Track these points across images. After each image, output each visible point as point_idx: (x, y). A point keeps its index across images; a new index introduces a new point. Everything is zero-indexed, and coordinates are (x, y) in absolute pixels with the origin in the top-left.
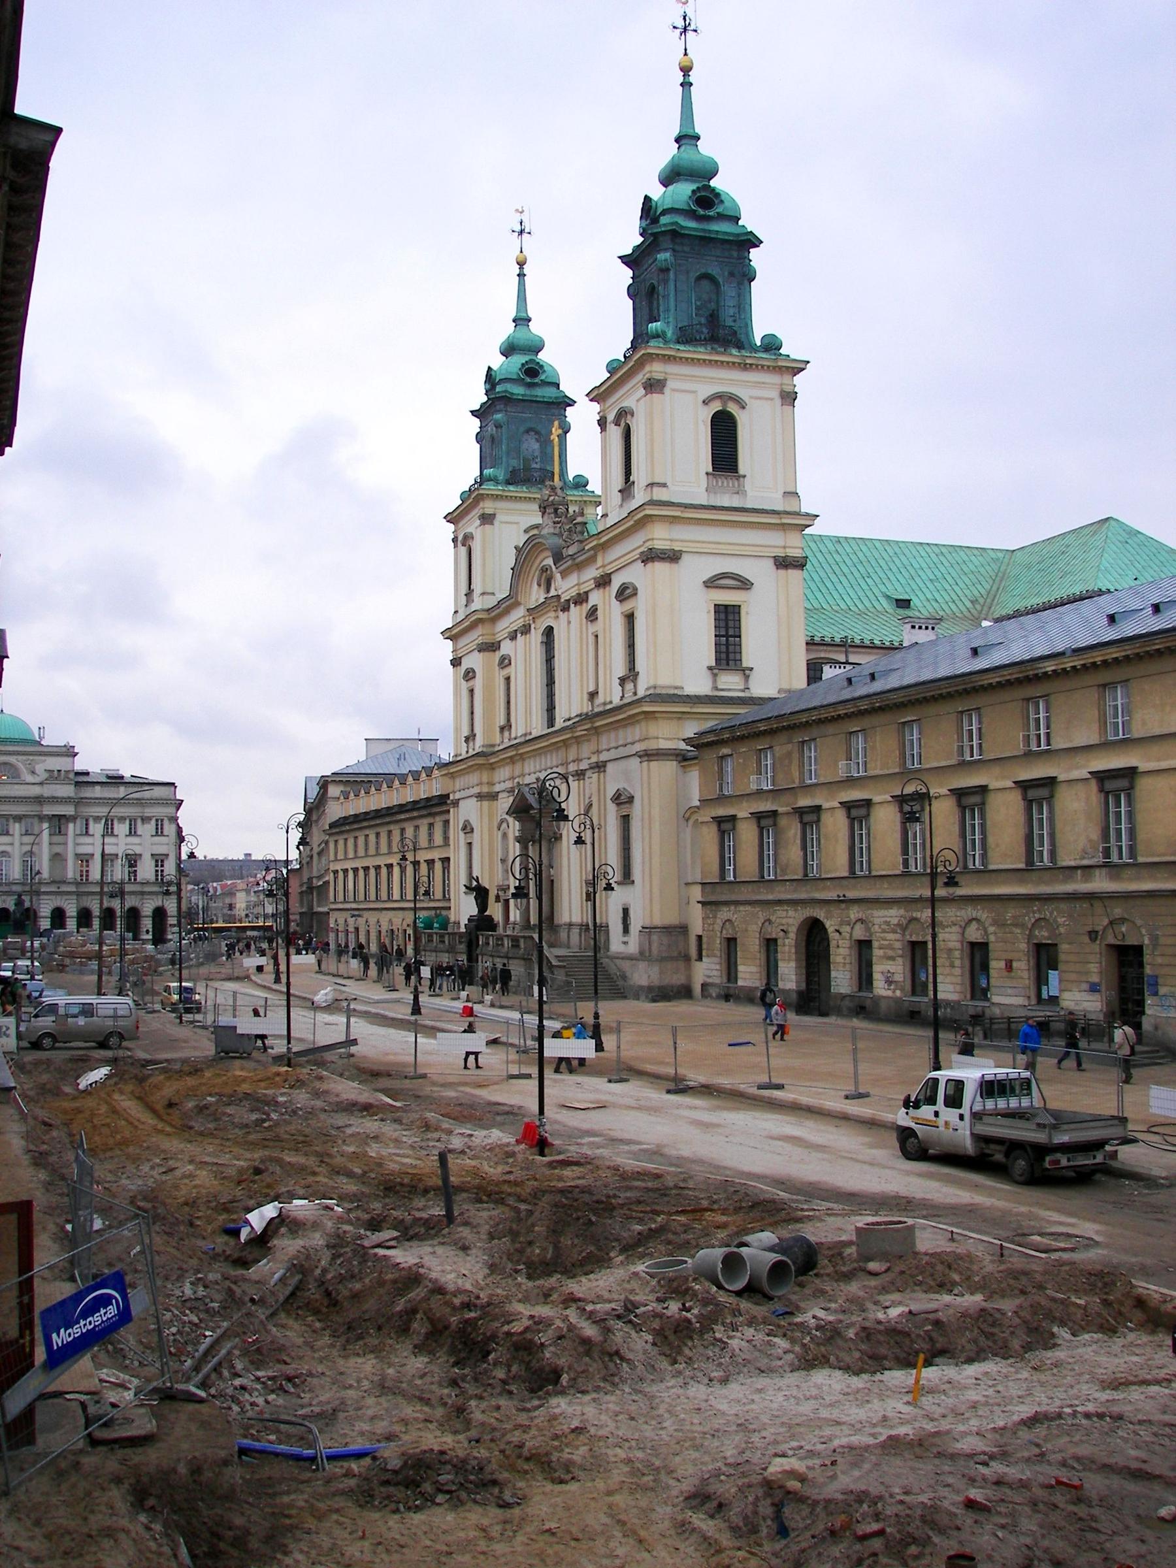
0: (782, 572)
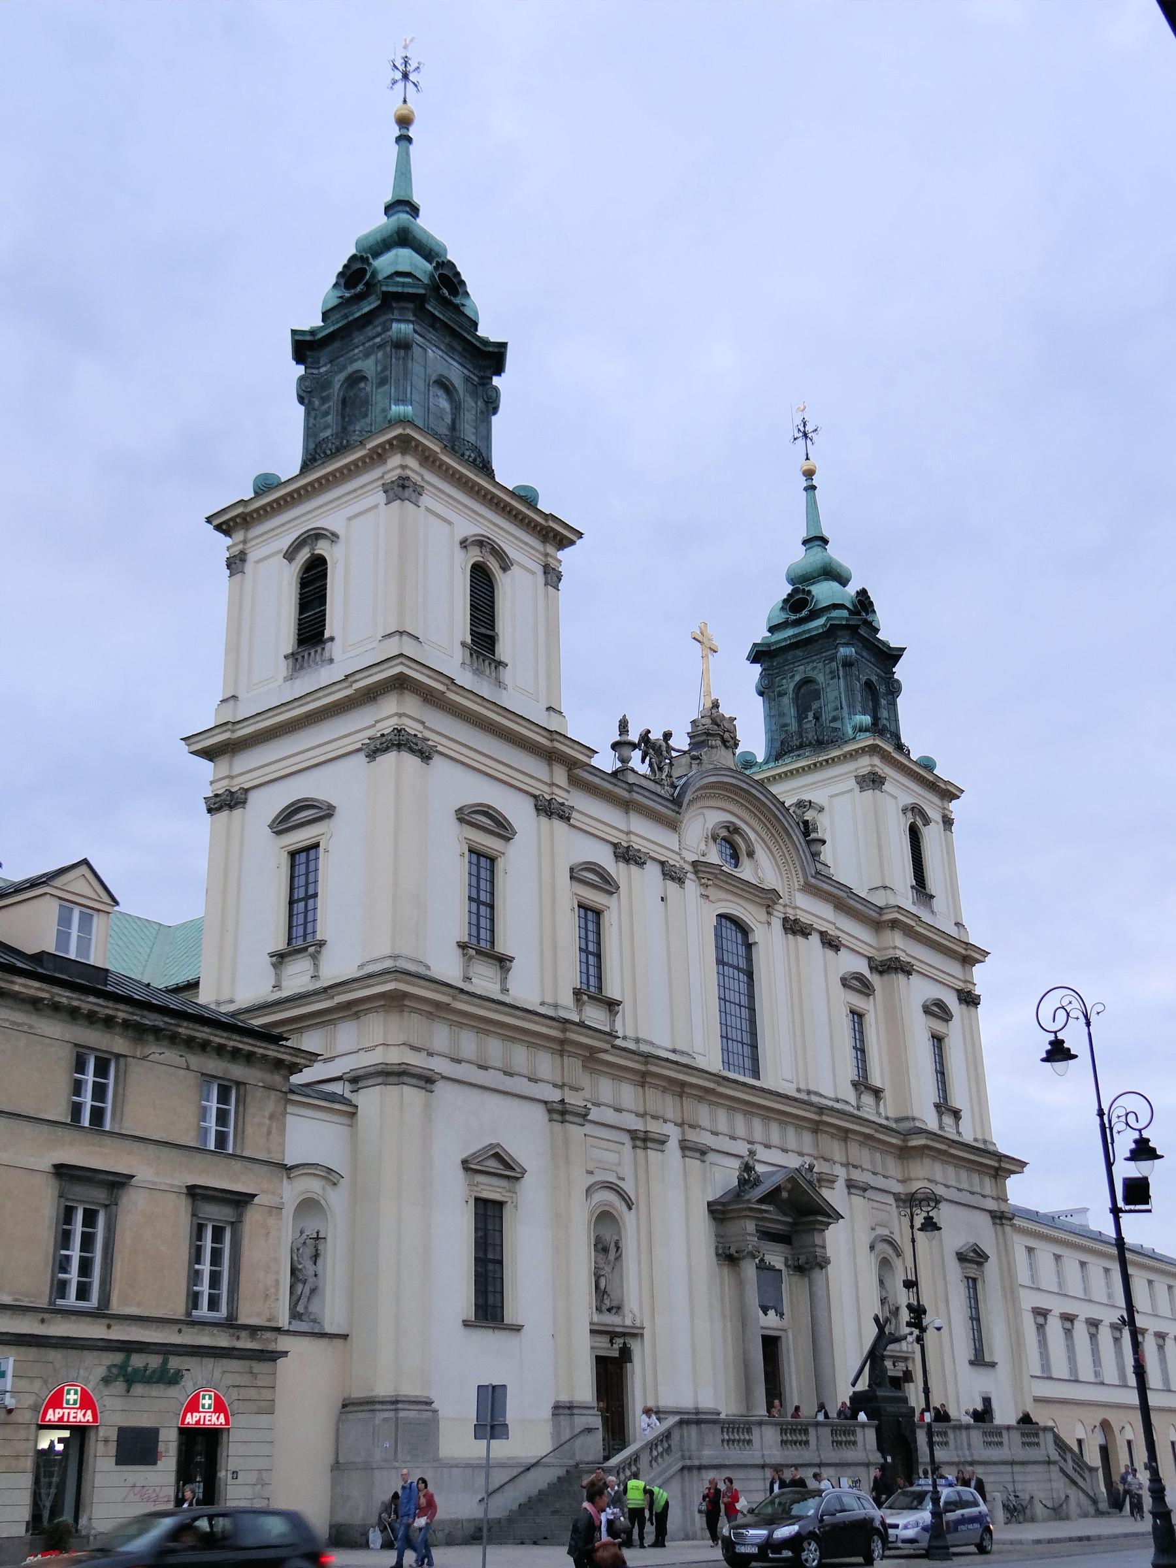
0: (544, 820)
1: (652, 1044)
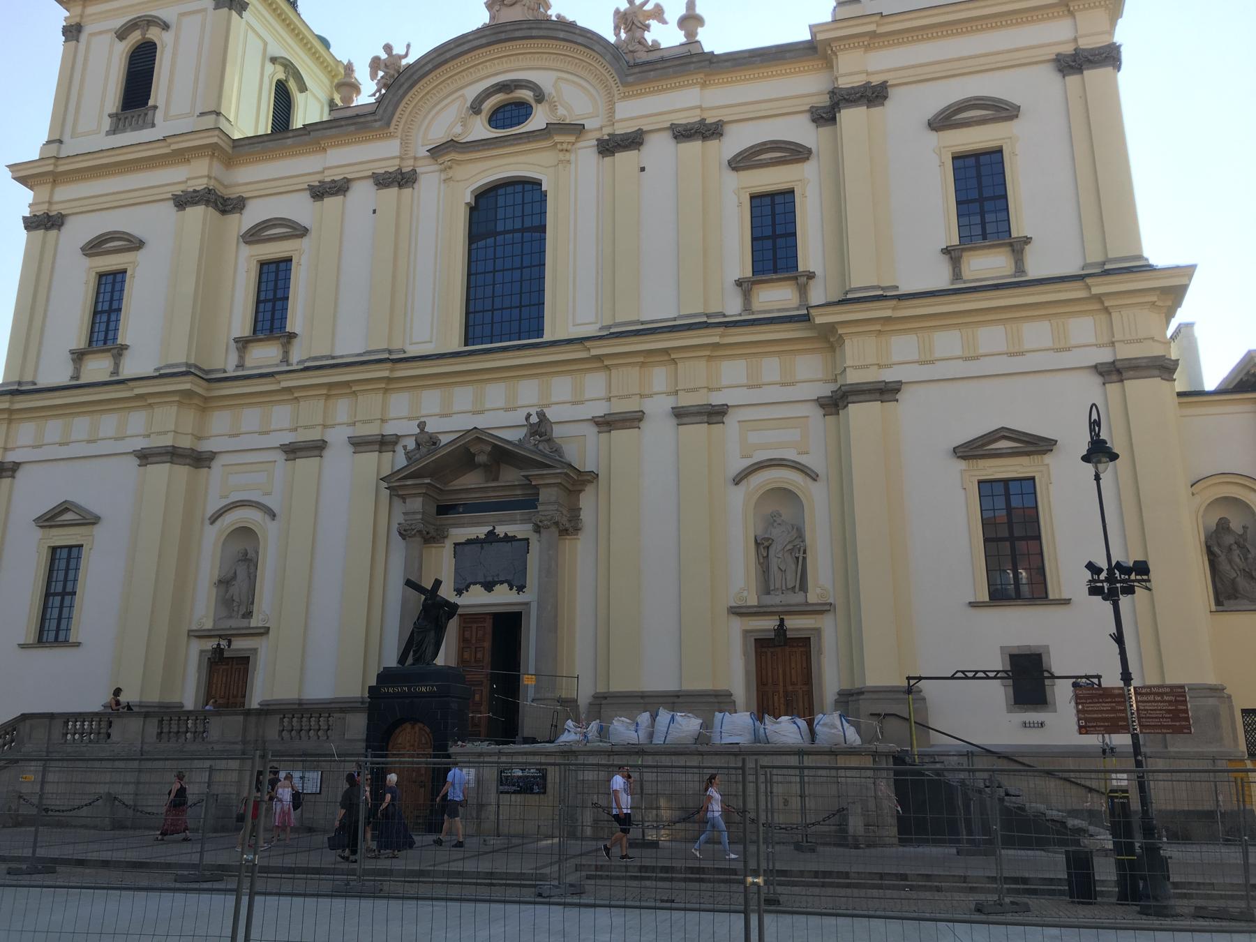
1: (333, 358)
